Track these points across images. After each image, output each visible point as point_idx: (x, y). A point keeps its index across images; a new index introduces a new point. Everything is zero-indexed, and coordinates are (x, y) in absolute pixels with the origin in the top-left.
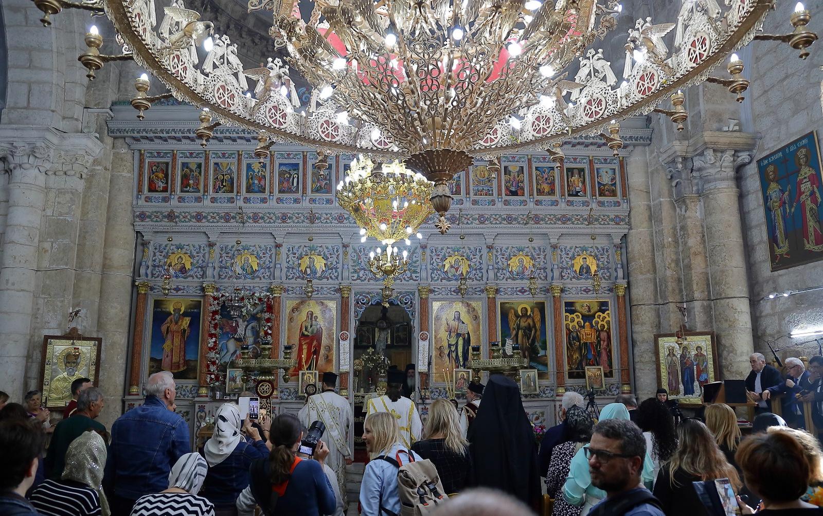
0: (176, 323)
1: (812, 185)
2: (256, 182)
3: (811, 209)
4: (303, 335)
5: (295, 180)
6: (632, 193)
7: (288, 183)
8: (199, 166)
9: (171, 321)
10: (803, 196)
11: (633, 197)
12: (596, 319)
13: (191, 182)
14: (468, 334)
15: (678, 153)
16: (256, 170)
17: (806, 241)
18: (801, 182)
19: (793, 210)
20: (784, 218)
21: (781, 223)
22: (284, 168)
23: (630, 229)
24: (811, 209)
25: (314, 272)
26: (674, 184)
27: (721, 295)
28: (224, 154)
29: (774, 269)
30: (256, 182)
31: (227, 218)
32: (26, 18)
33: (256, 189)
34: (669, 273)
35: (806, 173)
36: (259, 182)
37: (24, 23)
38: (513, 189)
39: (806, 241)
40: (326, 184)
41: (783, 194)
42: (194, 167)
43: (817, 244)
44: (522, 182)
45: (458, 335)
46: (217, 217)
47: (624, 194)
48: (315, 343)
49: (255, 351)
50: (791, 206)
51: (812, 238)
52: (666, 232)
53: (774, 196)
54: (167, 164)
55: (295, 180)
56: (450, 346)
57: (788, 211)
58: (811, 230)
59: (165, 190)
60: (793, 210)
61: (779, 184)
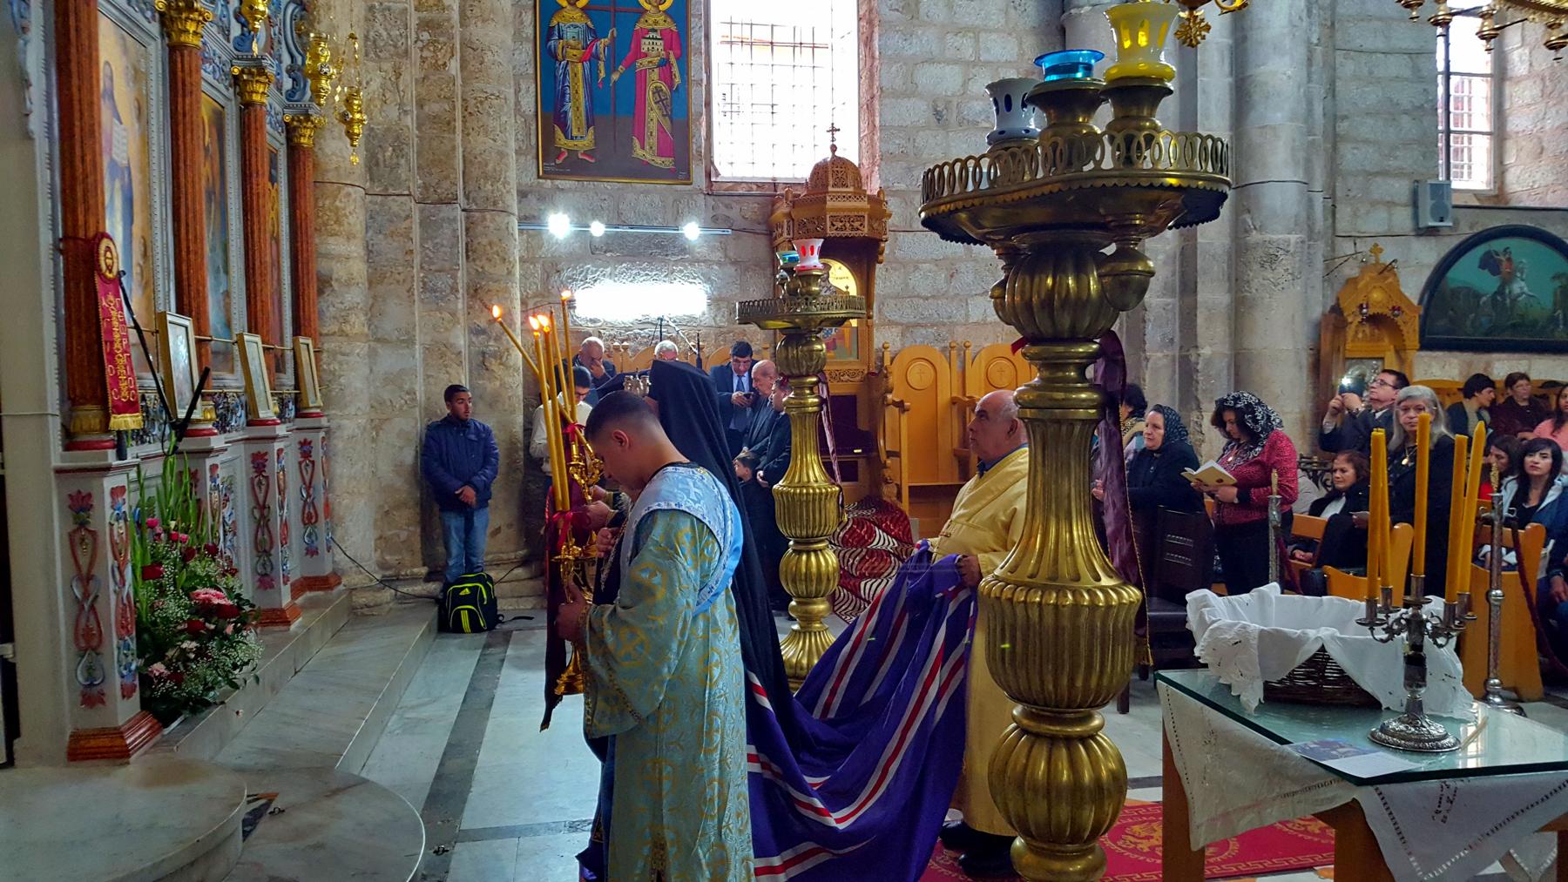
1: (668, 47)
3: (658, 91)
10: (645, 61)
14: (129, 168)
17: (636, 142)
18: (643, 34)
19: (615, 77)
20: (591, 82)
21: (581, 91)
24: (658, 91)
27: (495, 203)
29: (547, 175)
35: (656, 23)
39: (636, 142)
41: (596, 39)
43: (660, 154)
50: (609, 73)
51: (652, 141)
53: (570, 34)
57: (602, 75)
58: (652, 126)
60: (615, 77)
61: (589, 17)
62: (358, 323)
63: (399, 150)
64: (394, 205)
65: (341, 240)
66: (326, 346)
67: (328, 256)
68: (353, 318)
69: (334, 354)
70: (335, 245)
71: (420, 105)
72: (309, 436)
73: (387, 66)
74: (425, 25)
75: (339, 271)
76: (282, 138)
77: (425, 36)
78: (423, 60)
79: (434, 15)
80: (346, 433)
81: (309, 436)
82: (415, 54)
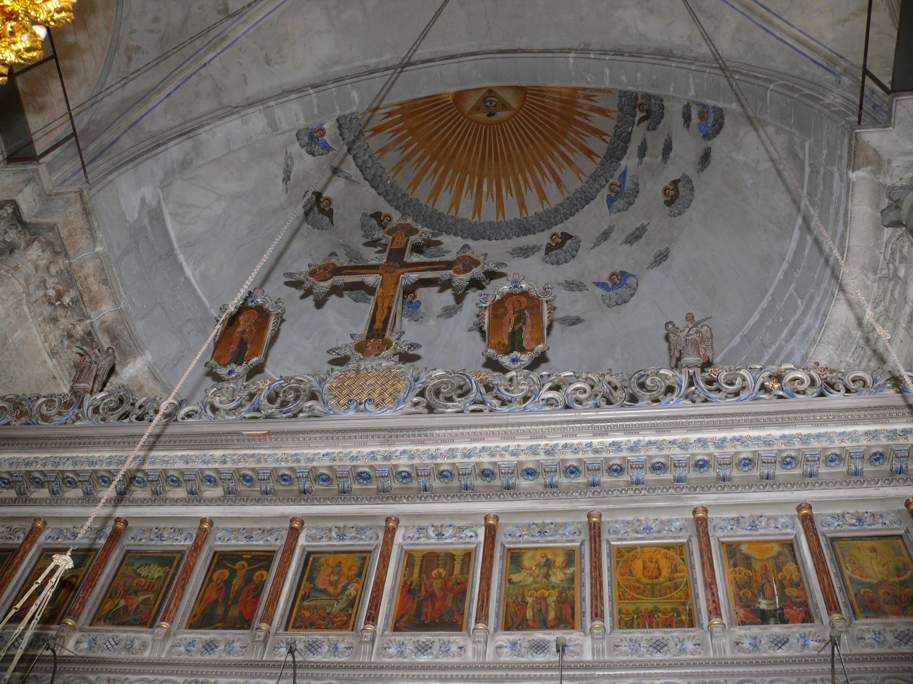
38: (763, 604)
40: (144, 602)
44: (799, 584)
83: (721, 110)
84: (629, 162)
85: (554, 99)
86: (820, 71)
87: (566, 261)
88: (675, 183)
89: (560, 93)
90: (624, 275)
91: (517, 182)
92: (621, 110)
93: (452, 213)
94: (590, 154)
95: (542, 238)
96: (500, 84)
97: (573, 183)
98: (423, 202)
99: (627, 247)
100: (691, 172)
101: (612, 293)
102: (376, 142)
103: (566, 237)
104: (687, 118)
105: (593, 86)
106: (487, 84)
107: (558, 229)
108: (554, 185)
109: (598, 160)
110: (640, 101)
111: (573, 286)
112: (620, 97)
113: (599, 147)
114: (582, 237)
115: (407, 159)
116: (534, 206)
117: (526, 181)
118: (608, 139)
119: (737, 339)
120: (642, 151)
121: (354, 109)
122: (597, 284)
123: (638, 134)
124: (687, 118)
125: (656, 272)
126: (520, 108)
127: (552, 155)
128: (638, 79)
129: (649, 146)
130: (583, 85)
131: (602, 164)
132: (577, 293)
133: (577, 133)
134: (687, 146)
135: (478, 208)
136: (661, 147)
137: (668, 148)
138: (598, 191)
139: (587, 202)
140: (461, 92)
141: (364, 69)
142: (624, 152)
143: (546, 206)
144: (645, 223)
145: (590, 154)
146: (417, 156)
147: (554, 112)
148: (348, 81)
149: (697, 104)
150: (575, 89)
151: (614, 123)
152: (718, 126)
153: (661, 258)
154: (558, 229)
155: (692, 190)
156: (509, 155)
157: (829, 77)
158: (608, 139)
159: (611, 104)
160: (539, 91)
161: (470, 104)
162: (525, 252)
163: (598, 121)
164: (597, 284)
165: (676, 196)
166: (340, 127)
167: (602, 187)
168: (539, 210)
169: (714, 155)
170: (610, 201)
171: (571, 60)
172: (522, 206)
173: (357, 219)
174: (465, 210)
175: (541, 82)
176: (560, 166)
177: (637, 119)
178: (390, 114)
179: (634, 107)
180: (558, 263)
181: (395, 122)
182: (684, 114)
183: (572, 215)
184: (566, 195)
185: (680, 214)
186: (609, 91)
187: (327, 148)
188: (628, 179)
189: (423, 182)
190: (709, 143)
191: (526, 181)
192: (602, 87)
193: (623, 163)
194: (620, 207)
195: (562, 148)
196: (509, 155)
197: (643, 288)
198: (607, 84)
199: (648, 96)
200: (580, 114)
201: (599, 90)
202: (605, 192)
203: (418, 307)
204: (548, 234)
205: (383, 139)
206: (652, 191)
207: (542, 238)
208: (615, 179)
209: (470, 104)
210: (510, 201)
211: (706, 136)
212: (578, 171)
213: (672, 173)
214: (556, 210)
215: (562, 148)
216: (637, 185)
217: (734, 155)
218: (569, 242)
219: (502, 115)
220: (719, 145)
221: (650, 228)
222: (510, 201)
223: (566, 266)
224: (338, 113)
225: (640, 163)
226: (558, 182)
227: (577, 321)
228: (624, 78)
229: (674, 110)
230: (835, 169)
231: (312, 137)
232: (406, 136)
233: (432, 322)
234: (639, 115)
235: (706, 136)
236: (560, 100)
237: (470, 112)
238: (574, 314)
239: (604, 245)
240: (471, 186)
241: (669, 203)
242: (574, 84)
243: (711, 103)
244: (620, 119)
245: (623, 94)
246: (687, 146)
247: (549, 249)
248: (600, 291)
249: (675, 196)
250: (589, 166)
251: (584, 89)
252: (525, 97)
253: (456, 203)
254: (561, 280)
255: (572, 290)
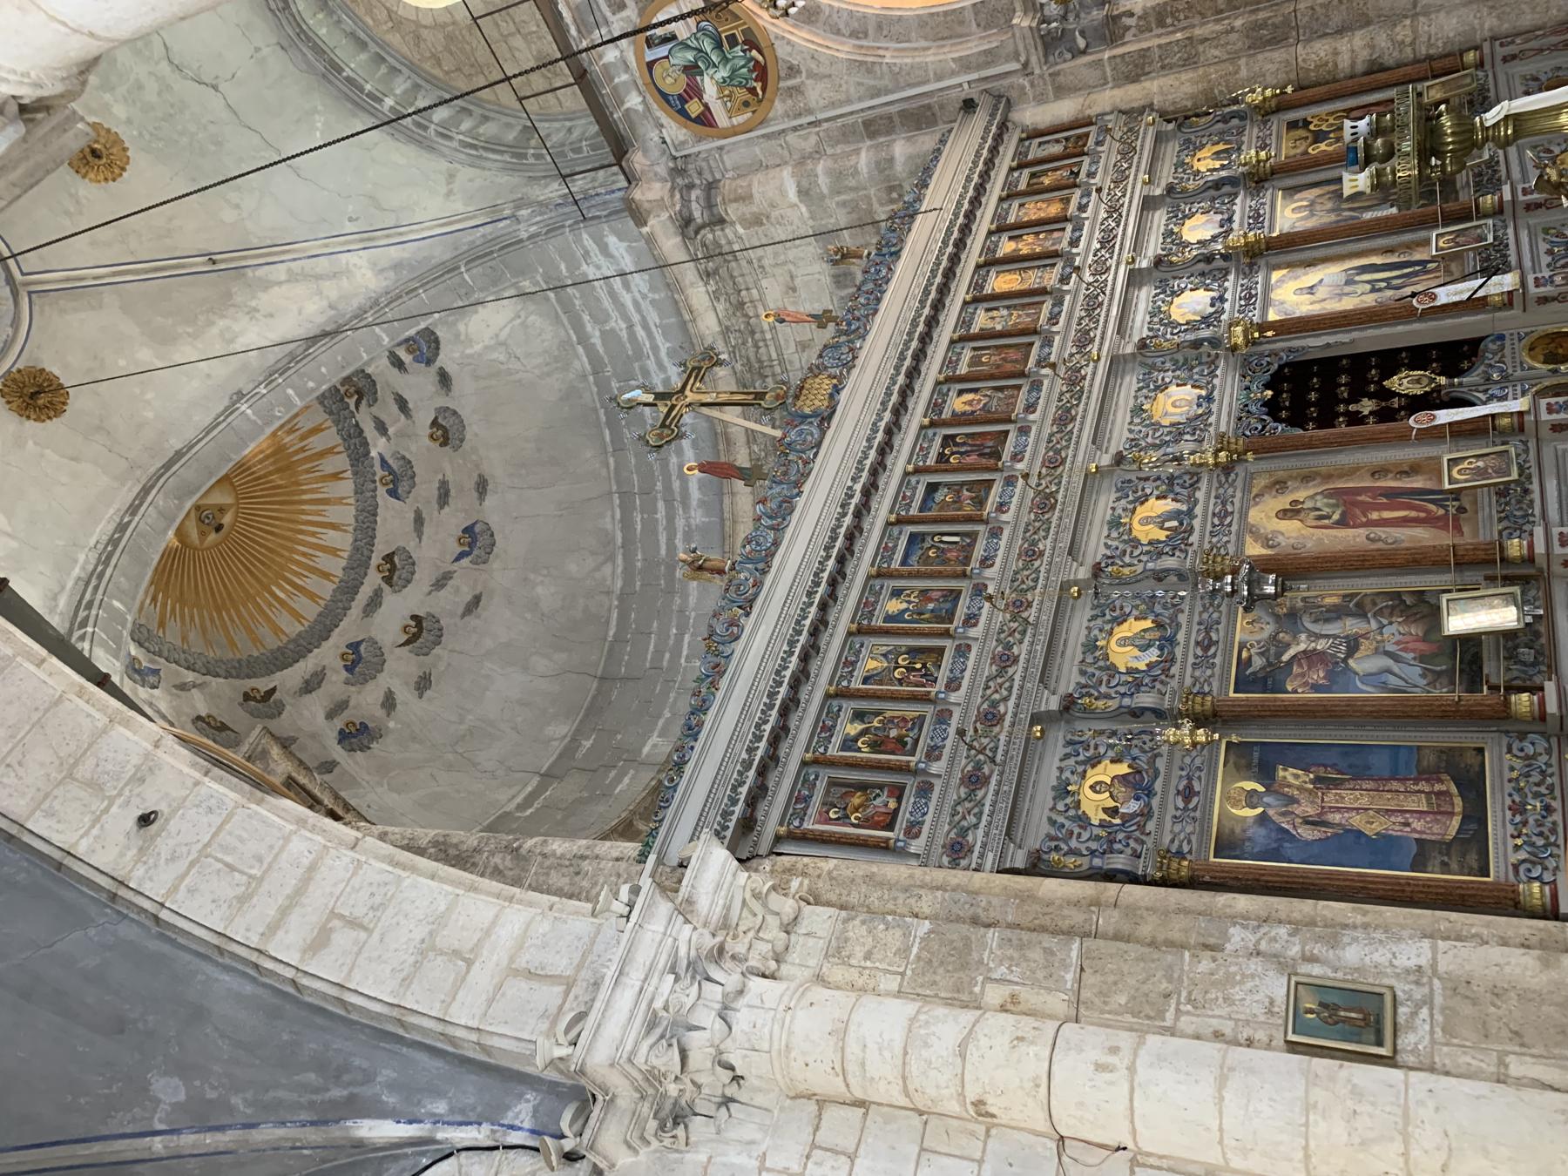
0: (1293, 800)
2: (931, 606)
4: (1343, 523)
5: (945, 539)
6: (1088, 112)
7: (950, 550)
8: (859, 716)
9: (1283, 814)
11: (1092, 112)
12: (1324, 128)
13: (893, 733)
15: (1034, 25)
16: (905, 605)
22: (914, 559)
23: (1151, 106)
25: (1176, 515)
26: (1081, 43)
28: (847, 663)
30: (931, 606)
31: (1005, 661)
32: (354, 923)
33: (948, 605)
34: (1238, 23)
36: (931, 600)
37: (363, 935)
42: (859, 727)
45: (1349, 282)
46: (997, 696)
47: (1089, 123)
48: (1362, 498)
49: (1387, 612)
52: (1163, 41)
54: (832, 783)
55: (945, 539)
56: (1373, 290)
59: (898, 792)
62: (1403, 32)
63: (1263, 25)
64: (1304, 20)
65: (1339, 59)
66: (1424, 52)
67: (1353, 64)
68: (1399, 38)
69: (1430, 46)
70: (1344, 62)
71: (1222, 11)
72: (1498, 59)
73: (1201, 48)
74: (1161, 23)
75: (1364, 55)
76: (1274, 119)
77: (1169, 21)
78: (1186, 18)
79: (1152, 19)
80: (1495, 22)
81: (1498, 59)
82: (1184, 24)
83: (427, 328)
84: (379, 447)
85: (260, 462)
86: (488, 228)
87: (413, 573)
88: (435, 423)
89: (261, 452)
90: (468, 530)
91: (298, 563)
92: (331, 413)
93: (285, 639)
94: (336, 476)
95: (373, 580)
96: (198, 495)
97: (346, 514)
98: (256, 654)
99: (447, 509)
100: (442, 401)
101: (476, 552)
102: (172, 634)
103: (389, 558)
104: (398, 364)
105: (287, 417)
106: (188, 505)
107: (376, 560)
108: (331, 533)
109: (349, 474)
110: (342, 390)
111: (441, 582)
112: (321, 403)
113: (341, 462)
114: (401, 544)
115: (204, 631)
116: (336, 566)
117: (304, 554)
118: (341, 449)
119: (611, 460)
120: (382, 428)
121: (129, 618)
122: (457, 559)
123: (364, 418)
124: (398, 364)
125: (490, 501)
126: (237, 499)
127: (303, 512)
128: (327, 369)
129: (383, 417)
130: (277, 424)
131: (355, 473)
132: (451, 582)
133: (308, 471)
134: (418, 385)
135: (297, 616)
136: (395, 408)
137: (402, 404)
138: (375, 497)
139: (375, 515)
140: (178, 529)
141: (82, 584)
142: (365, 444)
143: (345, 555)
144: (440, 477)
145: (336, 476)
146: (208, 623)
147: (271, 473)
148: (99, 596)
149: (399, 345)
150: (274, 434)
151: (334, 429)
152: (436, 342)
153: (482, 487)
154: (376, 560)
155: (455, 413)
156: (267, 548)
157: (501, 224)
158: (341, 449)
159: (319, 416)
160: (242, 467)
161: (194, 535)
162: (375, 602)
163: (317, 443)
164: (457, 559)
165: (445, 431)
166: (141, 645)
167: (375, 490)
168: (343, 563)
169: (451, 369)
170: (393, 493)
171: (249, 411)
172: (326, 575)
173: (241, 712)
174: (292, 628)
175: (236, 458)
176: (317, 513)
177: (352, 407)
178: (154, 599)
179: (342, 400)
180: (409, 582)
181: (164, 605)
182: (393, 364)
183: (373, 537)
184: (350, 529)
185: (462, 441)
186: (307, 407)
187: (156, 672)
188: (390, 462)
189: (236, 639)
190: (438, 364)
191: (304, 554)
192: (295, 411)
193: (373, 453)
194: (407, 488)
195: (305, 497)
196: (267, 548)
197: (494, 521)
198: (299, 403)
199: (347, 380)
200: (297, 452)
201: (296, 415)
202: (381, 491)
203: (366, 727)
204: (372, 572)
205: (174, 627)
206: (420, 446)
207: (373, 580)
208: (380, 473)
209: (194, 535)
210: (312, 582)
211: (429, 362)
212: (340, 501)
213: (424, 418)
214: (356, 549)
215: (305, 497)
216: (403, 458)
217: (468, 351)
218: (396, 559)
219: (227, 519)
220: (446, 359)
221: (450, 477)
222: (312, 582)
223: (416, 576)
224: (125, 633)
225: (389, 439)
226: (333, 526)
227: (477, 600)
228: (311, 384)
229: (380, 368)
230: (585, 267)
231: (136, 671)
232: (182, 609)
233: (391, 724)
234: (352, 402)
235: (429, 362)
236: (267, 457)
237: (202, 542)
238: (469, 598)
239: (427, 530)
240: (270, 605)
241: (444, 443)
242: (269, 431)
243: (412, 332)
244: (337, 422)
245: (321, 399)
246: (418, 385)
247: (388, 580)
248: (465, 562)
249: (445, 432)
250: (346, 487)
251: (282, 426)
252: (232, 484)
253: (277, 630)
254: (427, 589)
255: (443, 586)
